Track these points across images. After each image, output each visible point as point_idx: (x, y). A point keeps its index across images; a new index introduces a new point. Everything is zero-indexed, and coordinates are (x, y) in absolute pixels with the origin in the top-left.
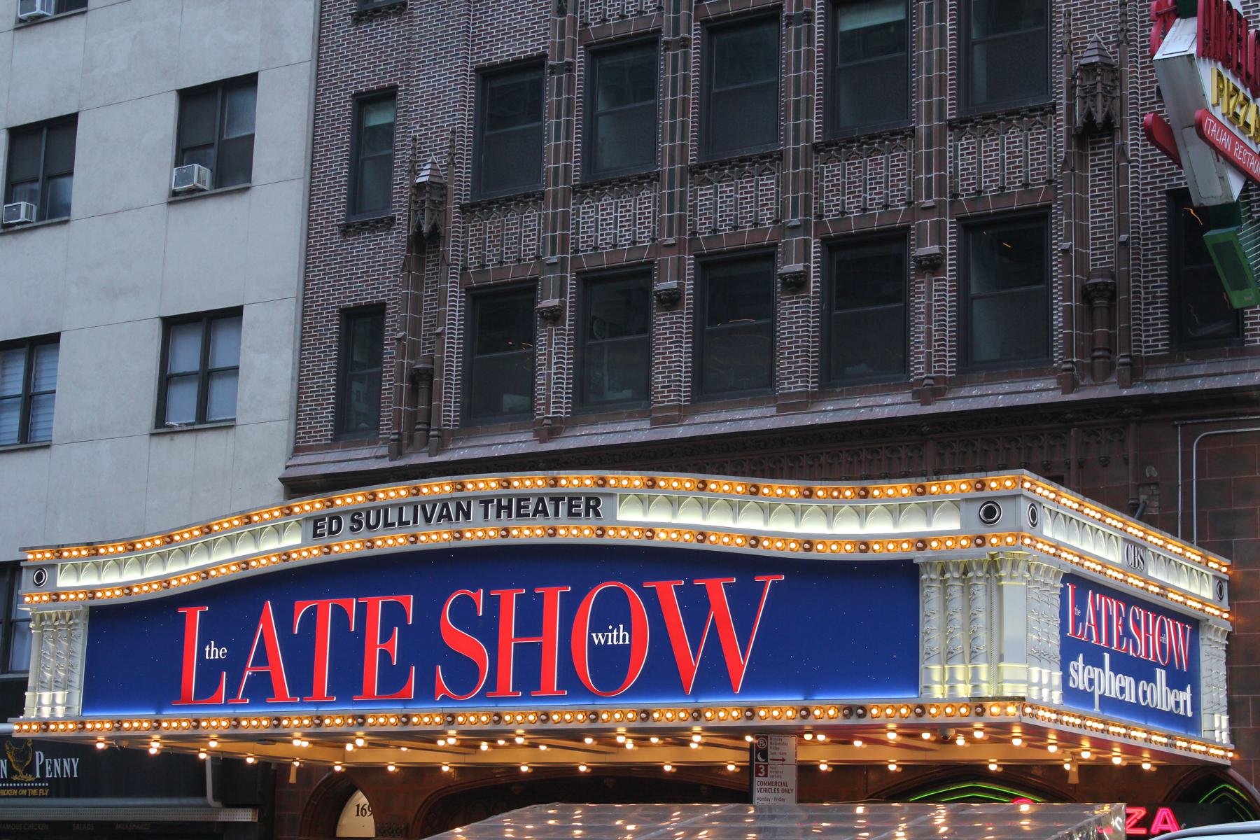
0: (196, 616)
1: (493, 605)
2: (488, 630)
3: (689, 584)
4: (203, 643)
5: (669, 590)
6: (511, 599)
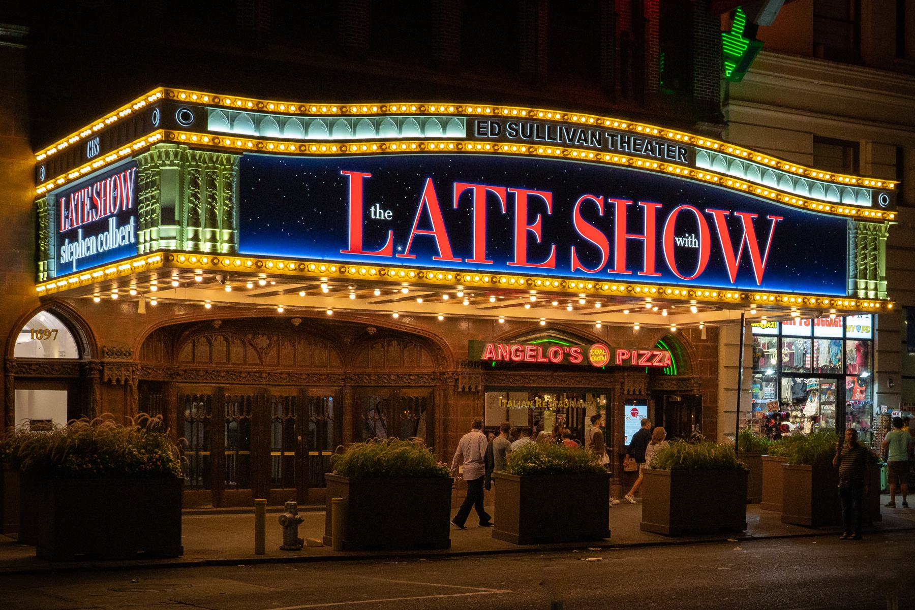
0: (355, 182)
1: (609, 209)
2: (606, 225)
3: (732, 215)
4: (367, 203)
5: (719, 216)
6: (620, 206)
